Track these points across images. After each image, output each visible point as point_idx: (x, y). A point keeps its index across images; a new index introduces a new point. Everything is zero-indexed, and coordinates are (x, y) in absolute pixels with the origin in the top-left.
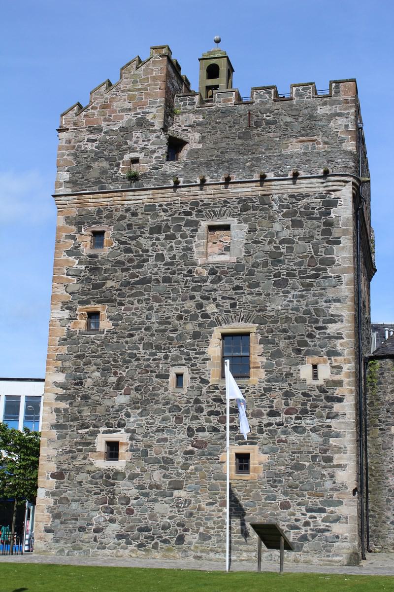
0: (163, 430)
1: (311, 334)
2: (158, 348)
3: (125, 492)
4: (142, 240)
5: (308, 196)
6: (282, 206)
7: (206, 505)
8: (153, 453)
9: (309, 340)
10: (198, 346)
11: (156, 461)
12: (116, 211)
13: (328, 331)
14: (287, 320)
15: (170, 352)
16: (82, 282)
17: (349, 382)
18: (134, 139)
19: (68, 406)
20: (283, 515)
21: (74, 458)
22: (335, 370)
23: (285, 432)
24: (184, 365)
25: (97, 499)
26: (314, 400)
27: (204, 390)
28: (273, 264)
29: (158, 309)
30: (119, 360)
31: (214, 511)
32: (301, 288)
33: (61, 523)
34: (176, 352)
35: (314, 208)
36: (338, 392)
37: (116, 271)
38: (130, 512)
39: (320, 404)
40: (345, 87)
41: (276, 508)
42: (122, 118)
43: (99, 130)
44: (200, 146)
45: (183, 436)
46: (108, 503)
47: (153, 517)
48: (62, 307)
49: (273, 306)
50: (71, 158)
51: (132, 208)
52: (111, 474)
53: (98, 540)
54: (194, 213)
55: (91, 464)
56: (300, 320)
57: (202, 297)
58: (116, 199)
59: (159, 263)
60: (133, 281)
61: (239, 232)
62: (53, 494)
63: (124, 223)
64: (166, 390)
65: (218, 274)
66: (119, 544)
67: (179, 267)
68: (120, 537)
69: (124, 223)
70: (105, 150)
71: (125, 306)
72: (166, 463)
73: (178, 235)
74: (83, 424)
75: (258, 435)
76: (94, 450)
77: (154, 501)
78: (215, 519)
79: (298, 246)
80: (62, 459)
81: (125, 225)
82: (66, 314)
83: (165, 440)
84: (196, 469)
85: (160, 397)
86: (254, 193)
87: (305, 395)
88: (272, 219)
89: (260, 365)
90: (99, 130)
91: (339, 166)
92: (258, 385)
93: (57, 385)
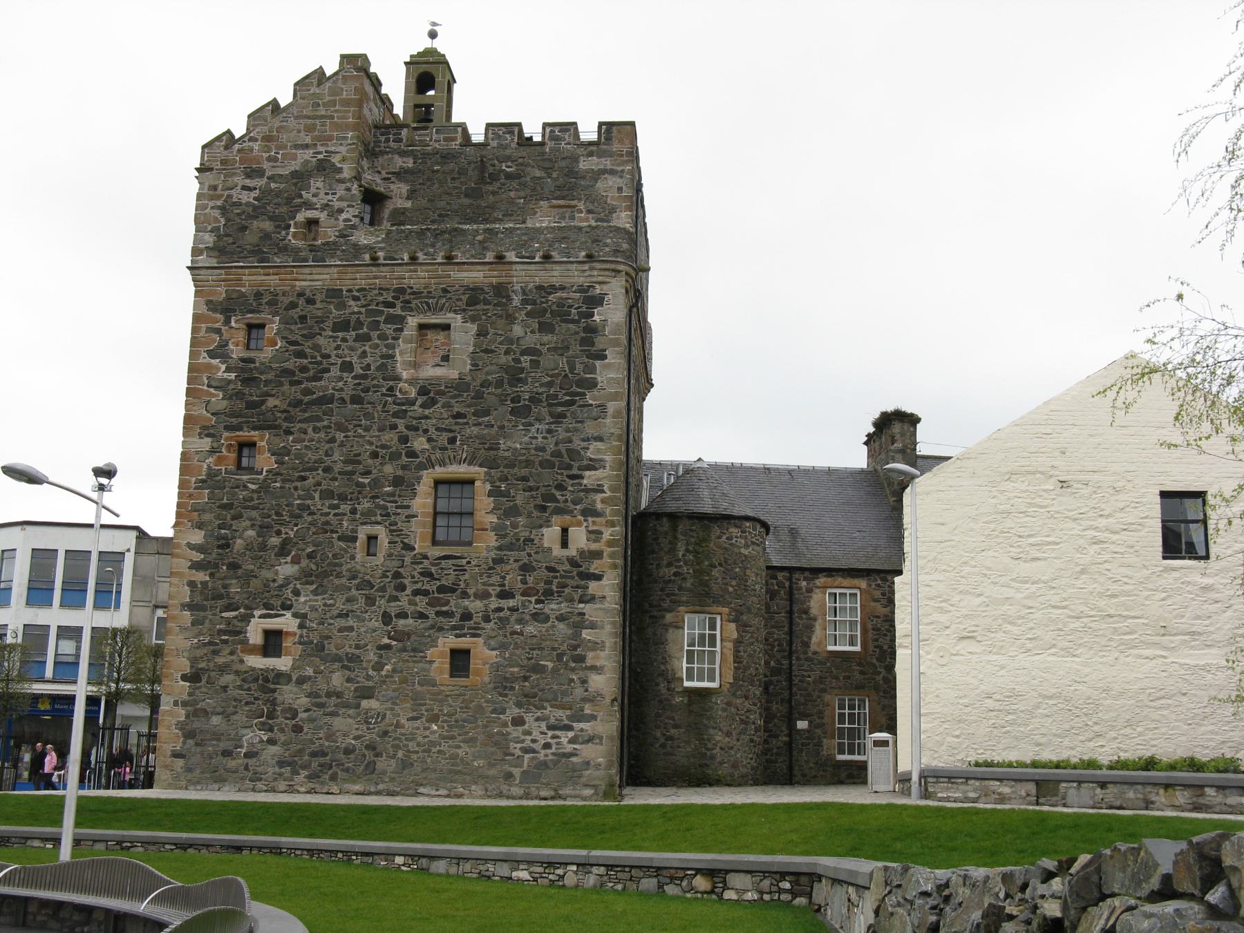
0: (347, 615)
2: (343, 498)
4: (321, 341)
5: (562, 288)
6: (525, 302)
8: (332, 647)
9: (558, 494)
10: (400, 496)
11: (337, 659)
12: (284, 295)
13: (585, 481)
14: (528, 463)
16: (230, 398)
17: (614, 553)
18: (313, 190)
19: (208, 578)
20: (515, 734)
21: (215, 653)
22: (593, 536)
23: (520, 621)
26: (562, 577)
27: (408, 560)
28: (511, 385)
31: (418, 728)
32: (548, 419)
33: (197, 744)
34: (368, 505)
35: (571, 307)
36: (595, 567)
37: (281, 384)
38: (298, 729)
39: (571, 582)
40: (619, 132)
41: (505, 725)
42: (294, 157)
43: (260, 173)
44: (409, 204)
45: (376, 624)
46: (268, 717)
47: (329, 737)
48: (200, 434)
49: (509, 443)
50: (217, 213)
51: (307, 292)
54: (399, 304)
55: (242, 661)
56: (546, 464)
57: (408, 427)
60: (307, 399)
61: (463, 334)
62: (185, 704)
64: (353, 558)
65: (432, 395)
66: (281, 775)
67: (375, 382)
68: (281, 764)
69: (294, 313)
72: (350, 662)
73: (375, 334)
74: (230, 605)
75: (483, 625)
76: (245, 642)
78: (420, 739)
79: (547, 361)
80: (199, 653)
81: (296, 316)
82: (206, 444)
83: (351, 629)
84: (394, 670)
85: (344, 568)
86: (486, 280)
87: (550, 569)
88: (511, 319)
90: (260, 173)
91: (607, 249)
92: (484, 554)
93: (191, 546)
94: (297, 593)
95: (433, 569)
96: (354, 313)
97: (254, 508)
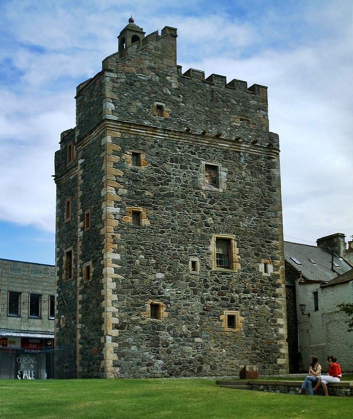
1: (263, 245)
2: (180, 243)
3: (165, 339)
4: (166, 166)
6: (246, 161)
7: (214, 347)
9: (262, 249)
14: (251, 234)
15: (187, 246)
16: (128, 189)
21: (130, 315)
22: (275, 269)
23: (253, 304)
24: (196, 256)
25: (148, 344)
27: (209, 273)
29: (178, 216)
30: (156, 248)
31: (218, 351)
35: (262, 166)
38: (169, 352)
52: (156, 327)
53: (150, 371)
57: (204, 212)
58: (148, 132)
59: (178, 184)
63: (154, 151)
65: (213, 198)
66: (163, 374)
67: (190, 189)
68: (164, 368)
69: (154, 151)
70: (139, 94)
71: (158, 211)
72: (189, 320)
75: (239, 305)
77: (184, 345)
80: (123, 315)
83: (188, 305)
84: (207, 324)
85: (184, 276)
87: (261, 282)
88: (240, 168)
89: (238, 261)
94: (164, 287)
95: (219, 279)
96: (179, 155)
97: (142, 245)
